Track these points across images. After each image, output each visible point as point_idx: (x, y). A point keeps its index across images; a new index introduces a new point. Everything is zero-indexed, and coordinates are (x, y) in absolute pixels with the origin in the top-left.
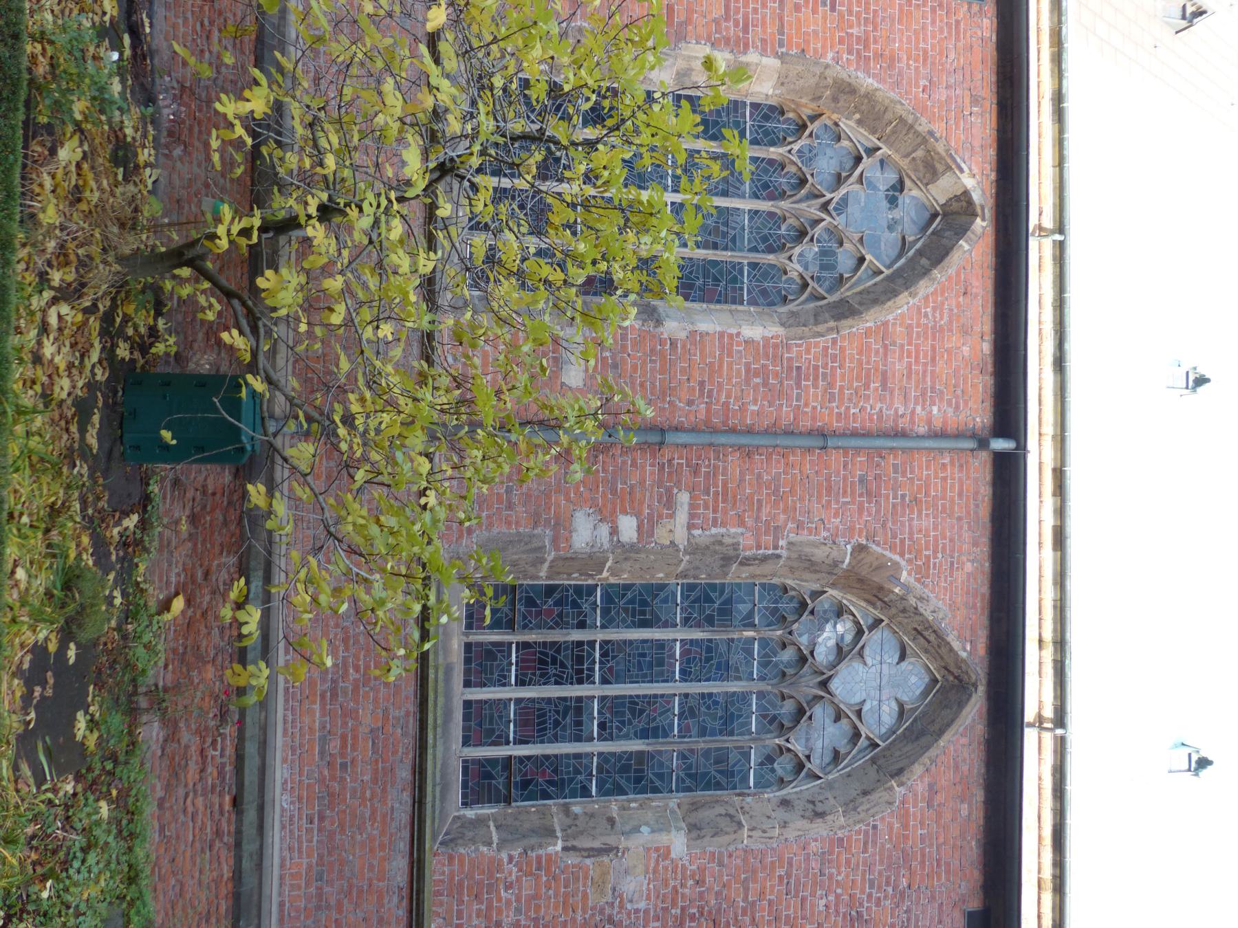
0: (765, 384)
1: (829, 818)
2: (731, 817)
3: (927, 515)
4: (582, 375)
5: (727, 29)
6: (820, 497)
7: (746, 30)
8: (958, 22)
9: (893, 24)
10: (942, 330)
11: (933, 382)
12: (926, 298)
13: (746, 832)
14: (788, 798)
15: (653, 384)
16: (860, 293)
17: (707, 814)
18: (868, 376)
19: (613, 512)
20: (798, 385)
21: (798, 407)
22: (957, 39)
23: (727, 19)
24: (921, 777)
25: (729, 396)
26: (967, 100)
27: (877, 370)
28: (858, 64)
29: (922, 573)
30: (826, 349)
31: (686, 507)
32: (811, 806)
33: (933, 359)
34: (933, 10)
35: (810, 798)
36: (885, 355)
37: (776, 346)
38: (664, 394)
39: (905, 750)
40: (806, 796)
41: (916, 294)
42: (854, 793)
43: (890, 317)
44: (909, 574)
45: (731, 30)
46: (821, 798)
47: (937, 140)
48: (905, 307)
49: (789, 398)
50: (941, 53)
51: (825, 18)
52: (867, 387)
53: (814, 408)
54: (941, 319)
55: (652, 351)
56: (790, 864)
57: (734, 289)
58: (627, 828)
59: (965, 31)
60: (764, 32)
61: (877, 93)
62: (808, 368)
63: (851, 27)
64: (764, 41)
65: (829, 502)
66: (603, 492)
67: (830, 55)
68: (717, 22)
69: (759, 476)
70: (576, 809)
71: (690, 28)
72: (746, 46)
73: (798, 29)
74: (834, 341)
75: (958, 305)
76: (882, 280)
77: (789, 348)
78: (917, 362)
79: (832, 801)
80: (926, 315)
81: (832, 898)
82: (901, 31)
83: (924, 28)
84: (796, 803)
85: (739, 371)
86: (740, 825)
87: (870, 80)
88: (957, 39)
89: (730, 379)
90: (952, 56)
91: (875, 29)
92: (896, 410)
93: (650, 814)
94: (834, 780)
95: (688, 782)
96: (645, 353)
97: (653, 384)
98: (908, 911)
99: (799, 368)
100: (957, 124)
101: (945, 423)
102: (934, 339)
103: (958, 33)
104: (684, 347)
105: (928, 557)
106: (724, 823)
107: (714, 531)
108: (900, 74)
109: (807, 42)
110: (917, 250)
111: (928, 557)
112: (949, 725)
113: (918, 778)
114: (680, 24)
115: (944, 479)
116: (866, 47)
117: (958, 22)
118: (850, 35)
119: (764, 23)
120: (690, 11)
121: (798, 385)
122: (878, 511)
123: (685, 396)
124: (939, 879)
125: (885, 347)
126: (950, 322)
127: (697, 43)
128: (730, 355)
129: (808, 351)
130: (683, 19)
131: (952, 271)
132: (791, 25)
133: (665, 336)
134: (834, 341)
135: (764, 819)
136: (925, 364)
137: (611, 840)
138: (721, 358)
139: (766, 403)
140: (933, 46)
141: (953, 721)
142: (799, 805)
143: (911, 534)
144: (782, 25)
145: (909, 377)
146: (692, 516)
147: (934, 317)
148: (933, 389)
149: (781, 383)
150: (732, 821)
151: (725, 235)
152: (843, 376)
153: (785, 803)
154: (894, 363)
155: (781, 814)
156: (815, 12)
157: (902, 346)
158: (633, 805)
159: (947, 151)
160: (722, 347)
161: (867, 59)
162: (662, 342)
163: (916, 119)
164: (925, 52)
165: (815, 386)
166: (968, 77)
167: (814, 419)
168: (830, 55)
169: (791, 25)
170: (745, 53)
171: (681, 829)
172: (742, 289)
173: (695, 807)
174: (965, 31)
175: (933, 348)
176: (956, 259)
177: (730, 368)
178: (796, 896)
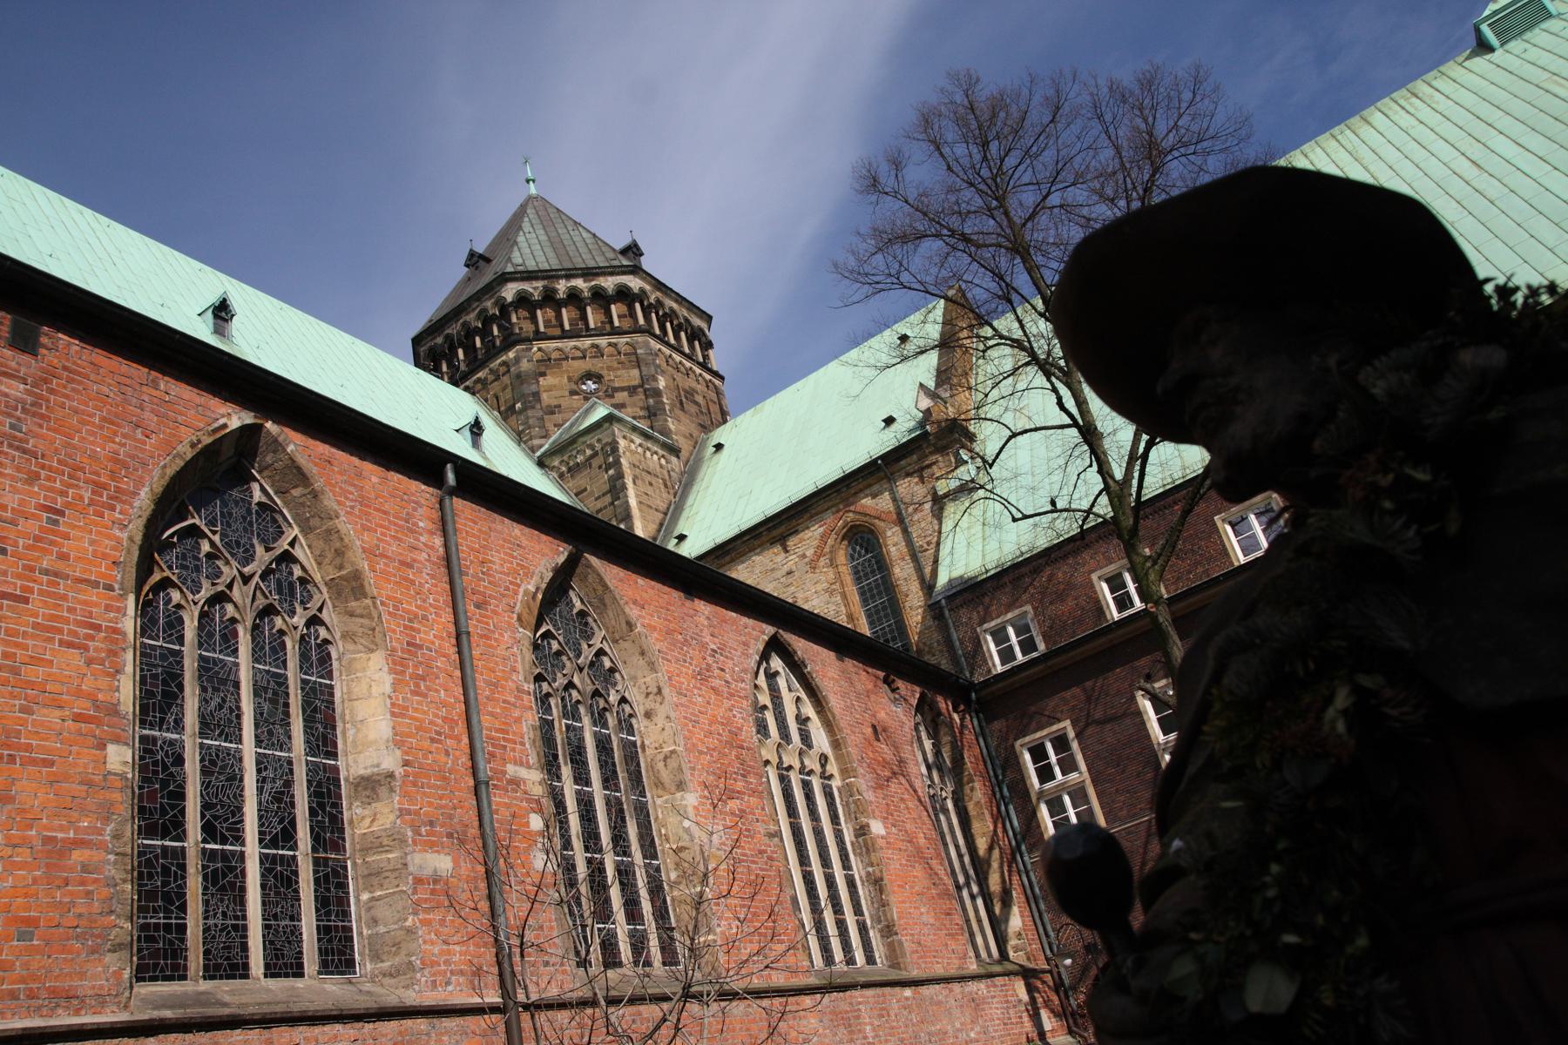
0: (423, 679)
1: (662, 684)
2: (665, 758)
3: (492, 556)
4: (442, 856)
5: (97, 650)
6: (491, 646)
7: (98, 628)
8: (65, 368)
9: (74, 447)
10: (362, 496)
11: (402, 519)
12: (339, 503)
13: (677, 748)
14: (643, 713)
15: (439, 787)
16: (319, 564)
17: (665, 776)
18: (406, 579)
19: (529, 833)
20: (421, 647)
21: (436, 651)
22: (86, 377)
23: (86, 649)
24: (631, 609)
25: (437, 716)
26: (154, 392)
27: (399, 570)
28: (124, 502)
29: (529, 575)
30: (389, 613)
31: (517, 768)
32: (651, 697)
33: (385, 513)
34: (52, 391)
35: (643, 696)
36: (387, 557)
37: (394, 663)
38: (445, 778)
39: (611, 615)
40: (641, 698)
41: (336, 511)
42: (642, 662)
43: (358, 543)
44: (529, 583)
45: (97, 645)
46: (644, 687)
47: (199, 441)
48: (349, 526)
49: (431, 659)
50: (105, 403)
51: (74, 527)
52: (412, 582)
53: (435, 636)
54: (352, 493)
55: (414, 784)
56: (685, 718)
57: (322, 693)
58: (686, 837)
59: (74, 363)
60: (97, 605)
61: (156, 491)
62: (407, 634)
63: (81, 498)
64: (108, 608)
65: (496, 640)
66: (519, 842)
67: (117, 533)
68: (89, 662)
69: (488, 698)
70: (673, 876)
71: (100, 696)
72: (116, 631)
73: (90, 562)
74: (383, 603)
75: (341, 473)
76: (306, 539)
77: (394, 650)
78: (389, 529)
79: (648, 679)
80: (352, 507)
81: (696, 691)
82: (82, 439)
83: (76, 411)
84: (648, 707)
85: (419, 703)
86: (673, 752)
87: (143, 494)
88: (86, 377)
89: (425, 713)
90: (105, 390)
91: (82, 470)
92: (426, 560)
93: (671, 820)
94: (628, 674)
95: (640, 788)
96: (417, 792)
97: (439, 787)
98: (692, 638)
99: (408, 644)
100: (181, 413)
101: (431, 520)
102: (369, 507)
103: (79, 374)
104: (406, 753)
105: (518, 564)
106: (673, 763)
107: (527, 746)
108: (132, 457)
109: (105, 556)
110: (276, 493)
111: (518, 564)
112: (601, 579)
113: (633, 612)
114: (97, 708)
115: (467, 532)
116: (104, 487)
117: (65, 368)
118: (92, 503)
119: (85, 603)
120: (79, 693)
121: (421, 647)
122: (495, 598)
123: (443, 757)
124: (673, 611)
125: (383, 556)
126: (354, 485)
127: (118, 690)
128: (406, 708)
129: (394, 631)
130: (89, 704)
131: (315, 470)
132: (85, 571)
133: (401, 770)
134: (383, 603)
135: (666, 733)
136: (390, 522)
137: (697, 848)
138: (411, 718)
139: (437, 681)
140: (96, 407)
141: (599, 575)
142: (649, 704)
143: (505, 574)
144: (86, 581)
145: (400, 540)
146: (521, 764)
147: (352, 500)
148: (407, 522)
149: (421, 663)
150: (670, 757)
151: (275, 693)
152: (409, 603)
153: (648, 715)
154: (393, 551)
155: (660, 720)
156: (66, 537)
157: (378, 539)
158: (663, 831)
159: (209, 435)
160: (403, 716)
161: (118, 489)
162: (407, 775)
163: (178, 455)
164: (103, 419)
165: (419, 631)
166: (128, 382)
167: (442, 638)
168: (117, 533)
169: (85, 571)
170: (126, 634)
171: (682, 796)
172: (320, 684)
173: (659, 784)
174: (74, 363)
175: (376, 510)
176: (302, 460)
177: (416, 710)
178: (698, 716)
